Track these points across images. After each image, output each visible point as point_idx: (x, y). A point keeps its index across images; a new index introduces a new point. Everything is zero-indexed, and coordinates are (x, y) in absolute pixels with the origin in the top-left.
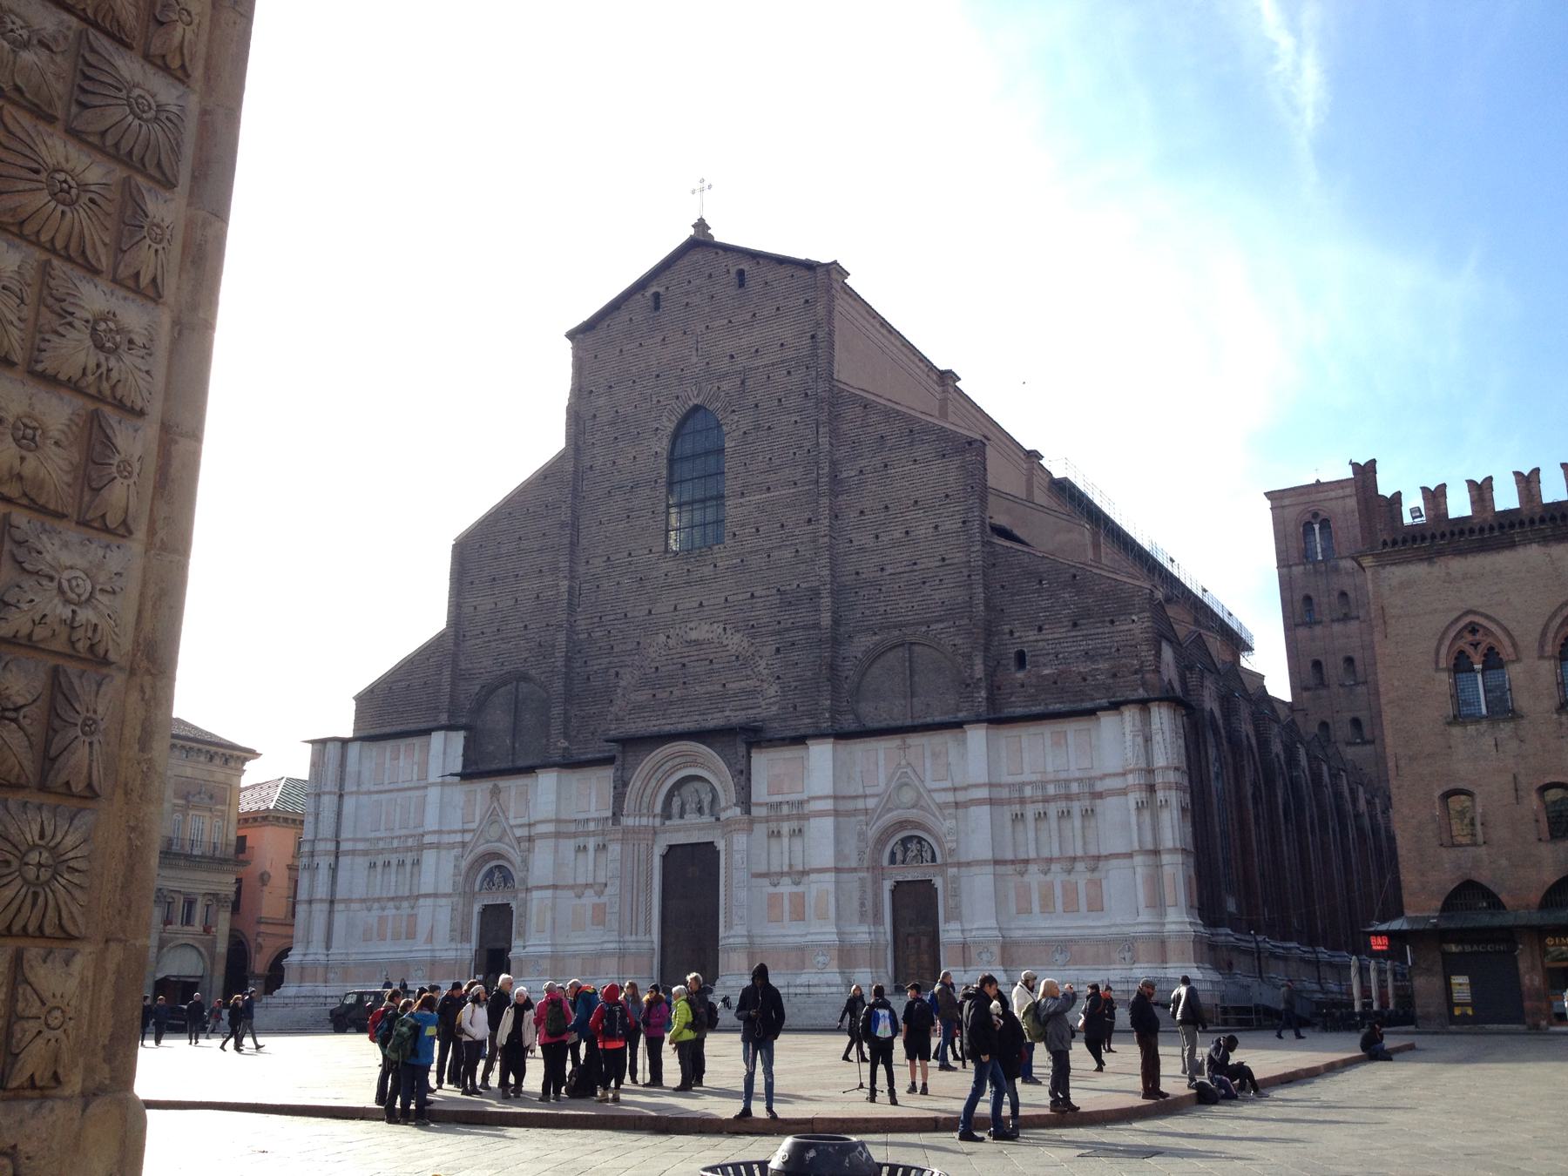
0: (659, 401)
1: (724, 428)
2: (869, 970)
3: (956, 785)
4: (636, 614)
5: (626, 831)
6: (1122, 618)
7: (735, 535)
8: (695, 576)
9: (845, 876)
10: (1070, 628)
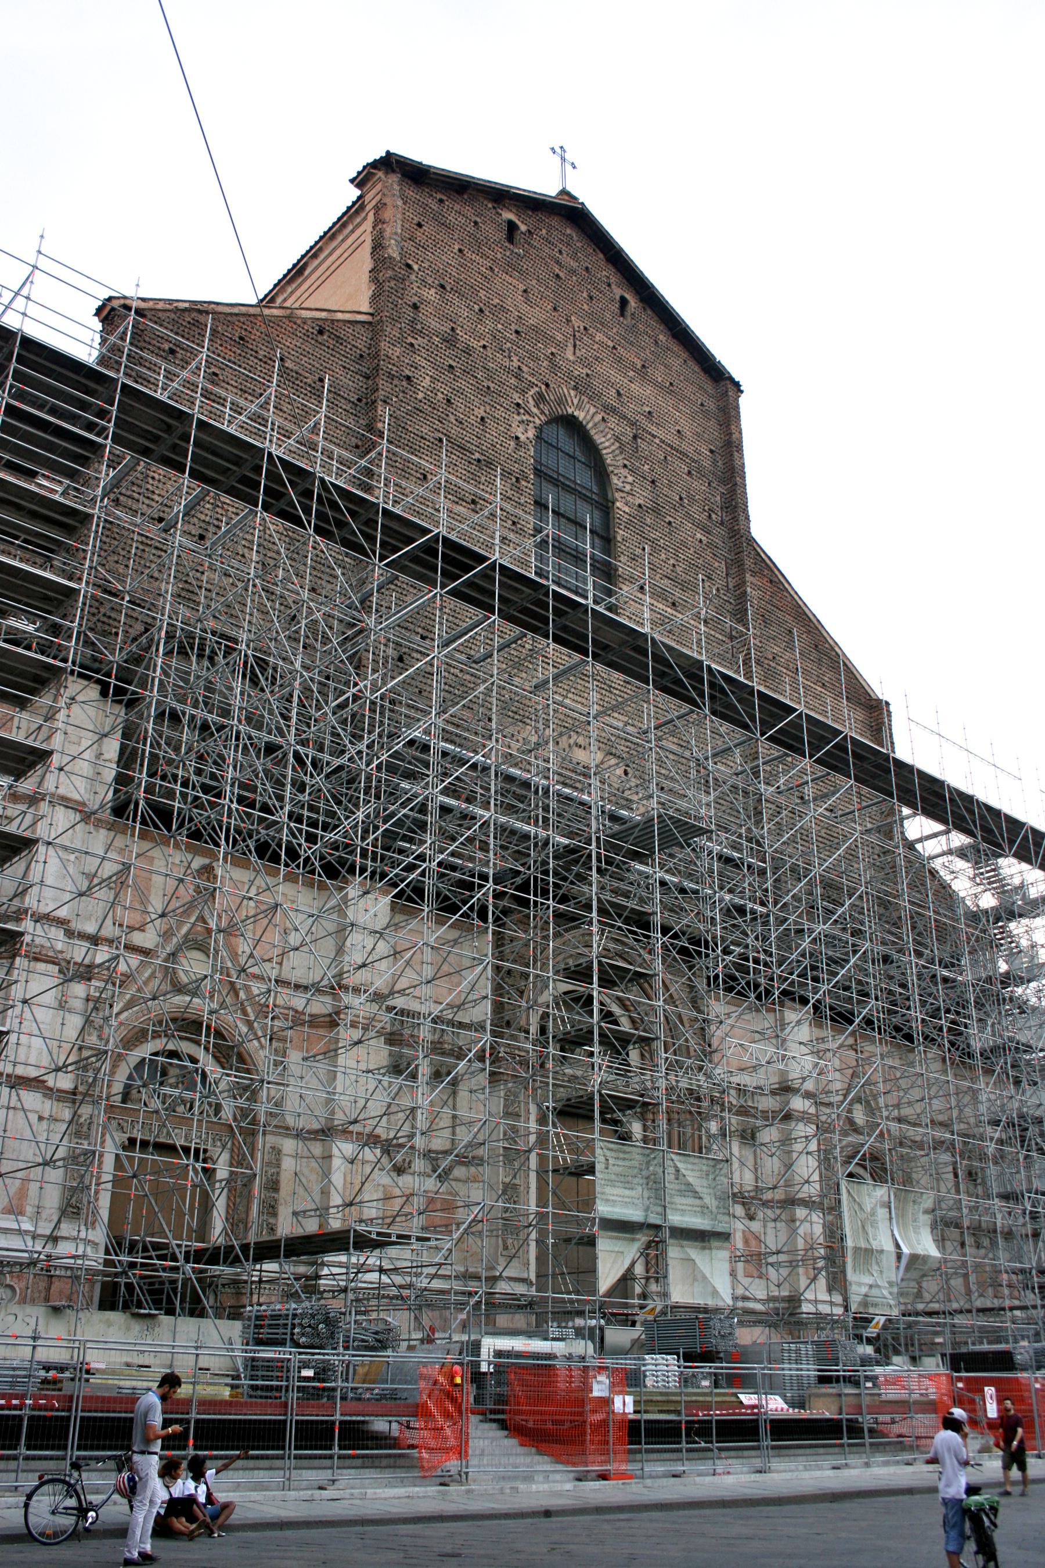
0: (519, 368)
1: (615, 480)
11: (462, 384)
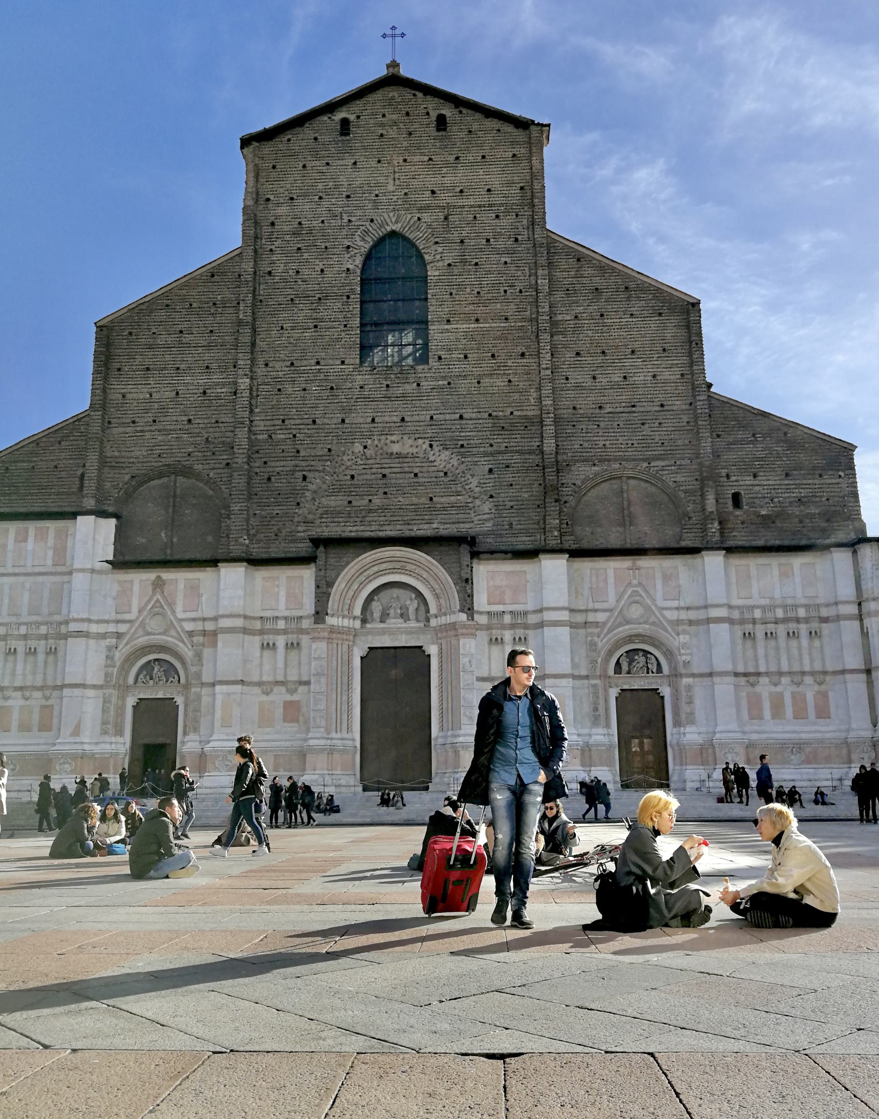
0: (350, 221)
1: (426, 257)
2: (606, 768)
3: (687, 605)
4: (326, 421)
5: (333, 630)
6: (831, 472)
7: (440, 358)
8: (400, 391)
9: (578, 683)
10: (783, 476)
11: (306, 255)
